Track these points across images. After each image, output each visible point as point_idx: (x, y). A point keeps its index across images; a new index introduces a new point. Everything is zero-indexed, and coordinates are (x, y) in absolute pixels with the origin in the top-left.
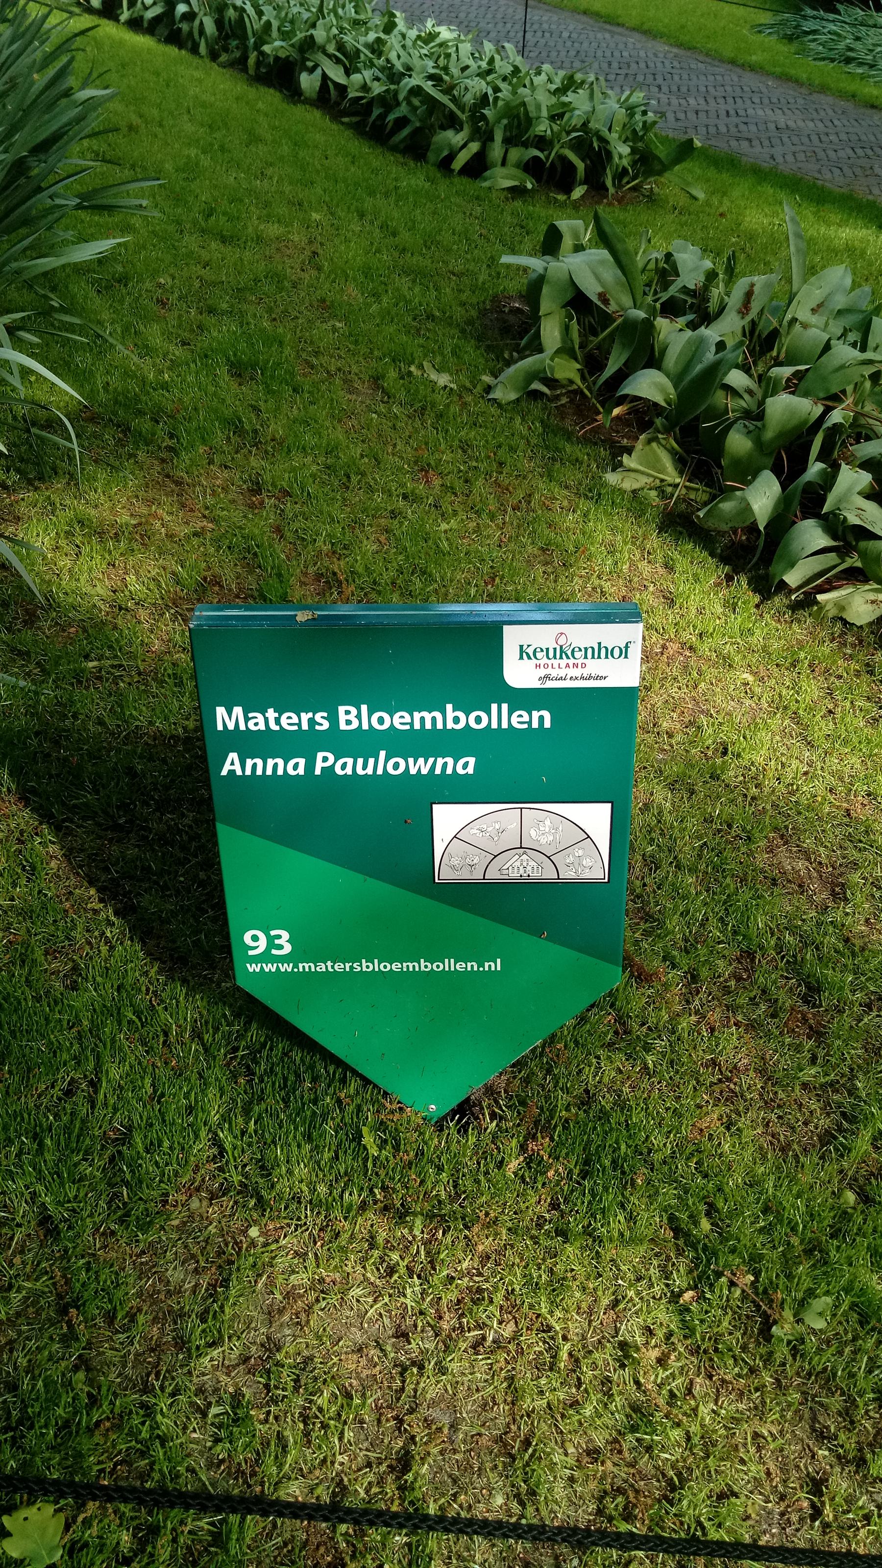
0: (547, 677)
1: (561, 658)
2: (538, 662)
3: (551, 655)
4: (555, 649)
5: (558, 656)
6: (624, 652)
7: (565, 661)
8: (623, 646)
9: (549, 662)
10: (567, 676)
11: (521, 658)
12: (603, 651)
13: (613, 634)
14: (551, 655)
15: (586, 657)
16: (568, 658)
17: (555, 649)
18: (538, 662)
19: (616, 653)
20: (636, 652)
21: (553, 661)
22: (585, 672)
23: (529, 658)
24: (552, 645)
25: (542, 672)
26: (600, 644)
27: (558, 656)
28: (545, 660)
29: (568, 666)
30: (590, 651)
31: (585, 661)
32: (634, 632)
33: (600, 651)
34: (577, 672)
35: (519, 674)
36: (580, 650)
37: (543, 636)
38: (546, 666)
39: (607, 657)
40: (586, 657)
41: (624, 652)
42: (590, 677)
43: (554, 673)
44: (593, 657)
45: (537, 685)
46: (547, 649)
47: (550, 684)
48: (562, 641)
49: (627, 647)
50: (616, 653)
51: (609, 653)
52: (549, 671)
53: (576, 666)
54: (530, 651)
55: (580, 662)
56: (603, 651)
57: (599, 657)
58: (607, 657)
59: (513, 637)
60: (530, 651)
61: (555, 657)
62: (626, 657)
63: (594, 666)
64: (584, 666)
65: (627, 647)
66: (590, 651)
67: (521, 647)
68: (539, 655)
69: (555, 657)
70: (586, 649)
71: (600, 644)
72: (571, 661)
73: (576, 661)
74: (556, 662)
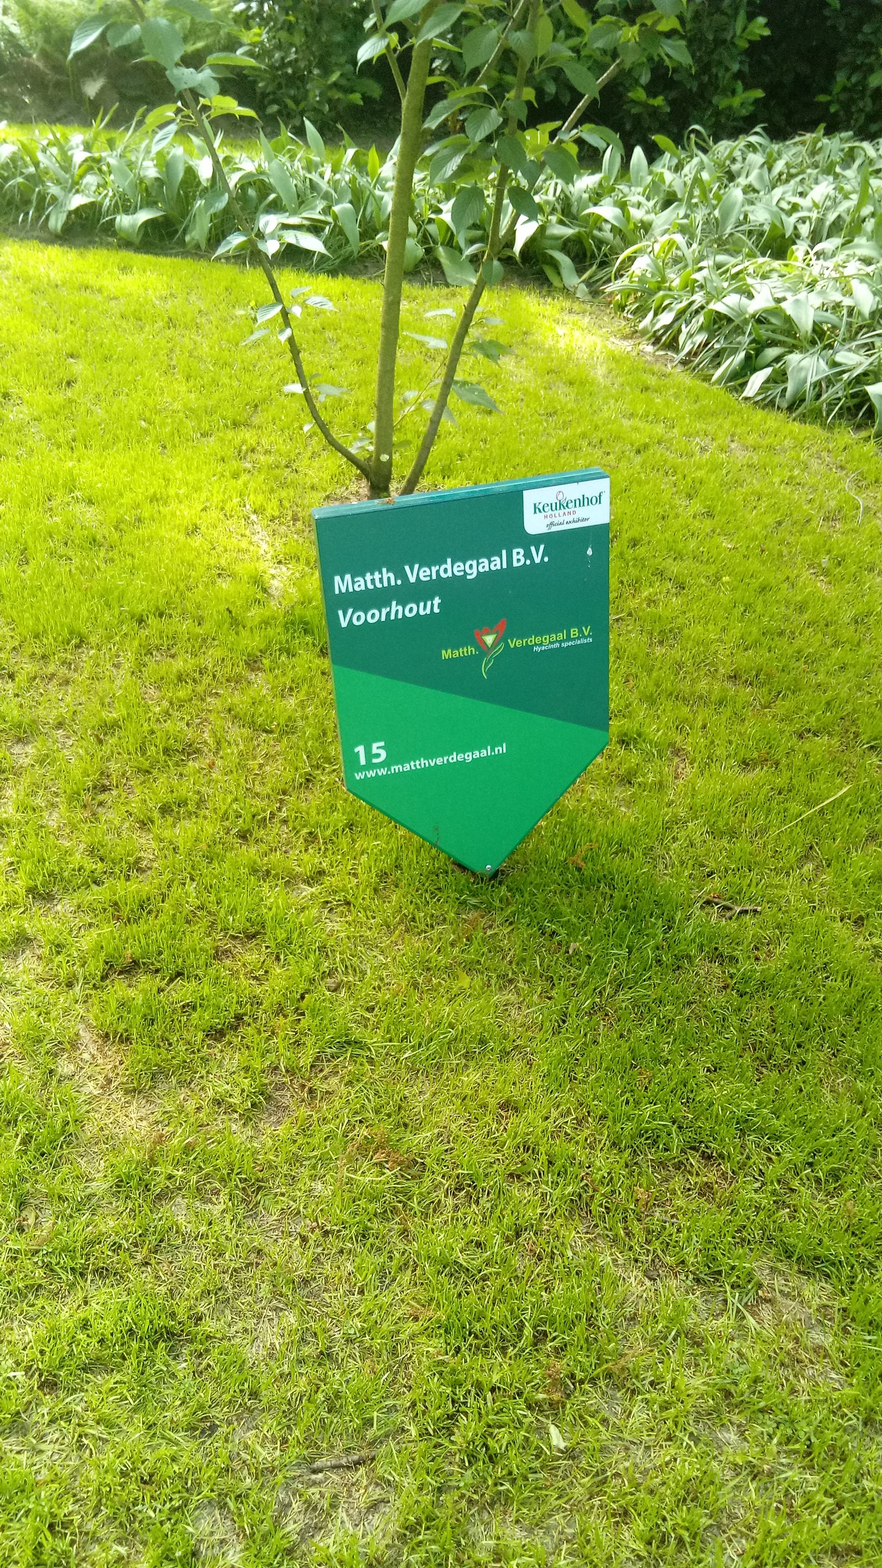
6: (599, 500)
10: (565, 521)
13: (590, 488)
20: (606, 499)
22: (576, 517)
25: (548, 521)
32: (603, 485)
34: (569, 518)
35: (534, 524)
37: (547, 495)
43: (556, 520)
45: (545, 530)
48: (560, 497)
51: (590, 501)
59: (530, 498)
63: (581, 512)
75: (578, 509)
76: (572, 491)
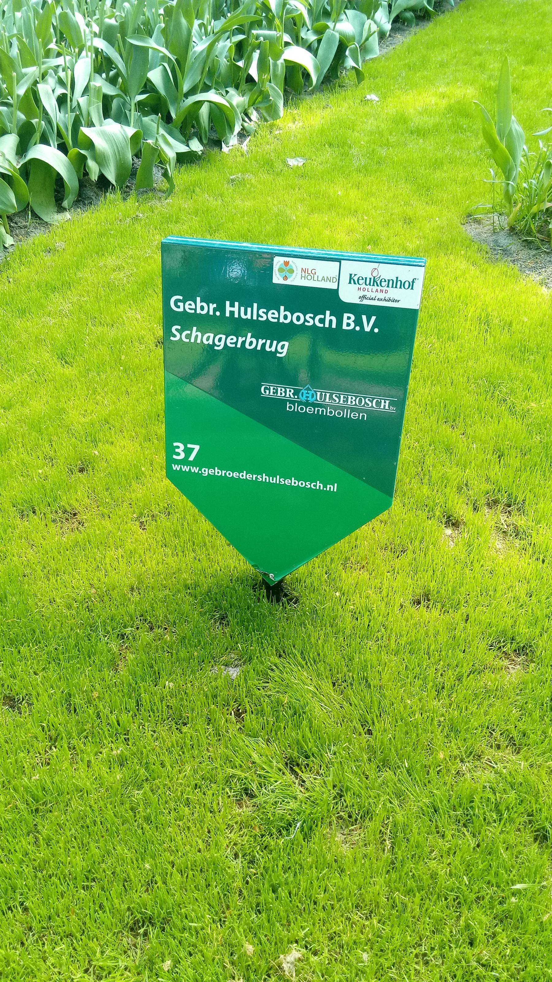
0: (364, 297)
1: (373, 285)
2: (360, 286)
3: (368, 283)
4: (370, 279)
5: (372, 284)
6: (411, 285)
7: (375, 288)
8: (411, 281)
9: (366, 287)
11: (350, 283)
12: (399, 283)
13: (405, 273)
14: (368, 283)
15: (388, 286)
16: (378, 286)
17: (370, 279)
18: (360, 286)
19: (407, 285)
20: (418, 286)
21: (369, 286)
22: (387, 296)
23: (355, 283)
24: (369, 276)
25: (362, 293)
26: (397, 278)
27: (372, 284)
28: (364, 286)
29: (377, 291)
30: (391, 282)
31: (387, 289)
32: (418, 273)
36: (385, 281)
38: (364, 289)
39: (400, 288)
40: (388, 286)
42: (389, 300)
43: (369, 295)
44: (392, 287)
45: (357, 301)
46: (366, 278)
47: (365, 302)
48: (375, 274)
49: (413, 282)
50: (407, 285)
51: (402, 285)
52: (366, 293)
53: (382, 291)
54: (356, 278)
55: (384, 289)
56: (399, 283)
57: (396, 287)
58: (400, 288)
60: (356, 278)
61: (370, 284)
62: (412, 289)
63: (393, 293)
64: (386, 292)
65: (413, 282)
66: (391, 282)
67: (351, 275)
68: (361, 282)
69: (370, 284)
70: (389, 281)
71: (397, 278)
72: (379, 288)
73: (382, 288)
74: (370, 288)
75: (390, 289)
76: (388, 272)
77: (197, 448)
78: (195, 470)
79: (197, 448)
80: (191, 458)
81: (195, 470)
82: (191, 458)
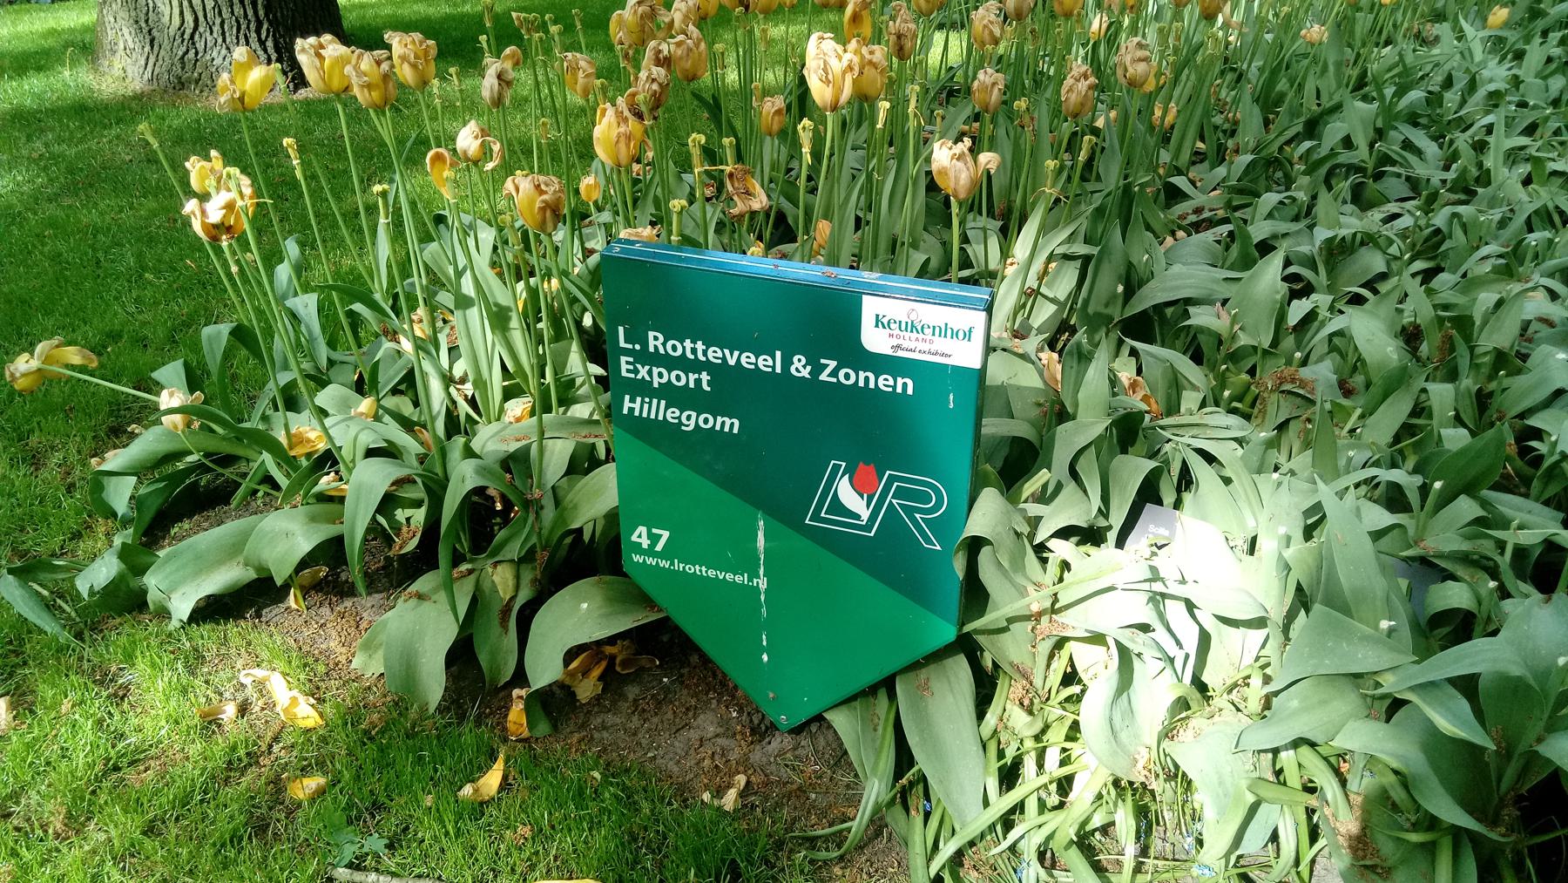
0: (898, 347)
6: (968, 335)
7: (914, 335)
10: (917, 348)
19: (961, 335)
22: (933, 348)
25: (895, 342)
28: (897, 332)
33: (944, 331)
34: (925, 347)
35: (874, 340)
38: (898, 337)
41: (968, 335)
42: (936, 354)
43: (906, 344)
45: (890, 352)
47: (900, 354)
48: (913, 317)
50: (961, 335)
51: (955, 334)
52: (900, 342)
59: (871, 307)
60: (885, 321)
63: (941, 344)
72: (921, 336)
75: (936, 338)
77: (666, 534)
78: (664, 564)
79: (666, 534)
80: (659, 548)
81: (664, 564)
82: (659, 548)
